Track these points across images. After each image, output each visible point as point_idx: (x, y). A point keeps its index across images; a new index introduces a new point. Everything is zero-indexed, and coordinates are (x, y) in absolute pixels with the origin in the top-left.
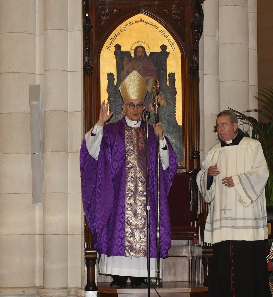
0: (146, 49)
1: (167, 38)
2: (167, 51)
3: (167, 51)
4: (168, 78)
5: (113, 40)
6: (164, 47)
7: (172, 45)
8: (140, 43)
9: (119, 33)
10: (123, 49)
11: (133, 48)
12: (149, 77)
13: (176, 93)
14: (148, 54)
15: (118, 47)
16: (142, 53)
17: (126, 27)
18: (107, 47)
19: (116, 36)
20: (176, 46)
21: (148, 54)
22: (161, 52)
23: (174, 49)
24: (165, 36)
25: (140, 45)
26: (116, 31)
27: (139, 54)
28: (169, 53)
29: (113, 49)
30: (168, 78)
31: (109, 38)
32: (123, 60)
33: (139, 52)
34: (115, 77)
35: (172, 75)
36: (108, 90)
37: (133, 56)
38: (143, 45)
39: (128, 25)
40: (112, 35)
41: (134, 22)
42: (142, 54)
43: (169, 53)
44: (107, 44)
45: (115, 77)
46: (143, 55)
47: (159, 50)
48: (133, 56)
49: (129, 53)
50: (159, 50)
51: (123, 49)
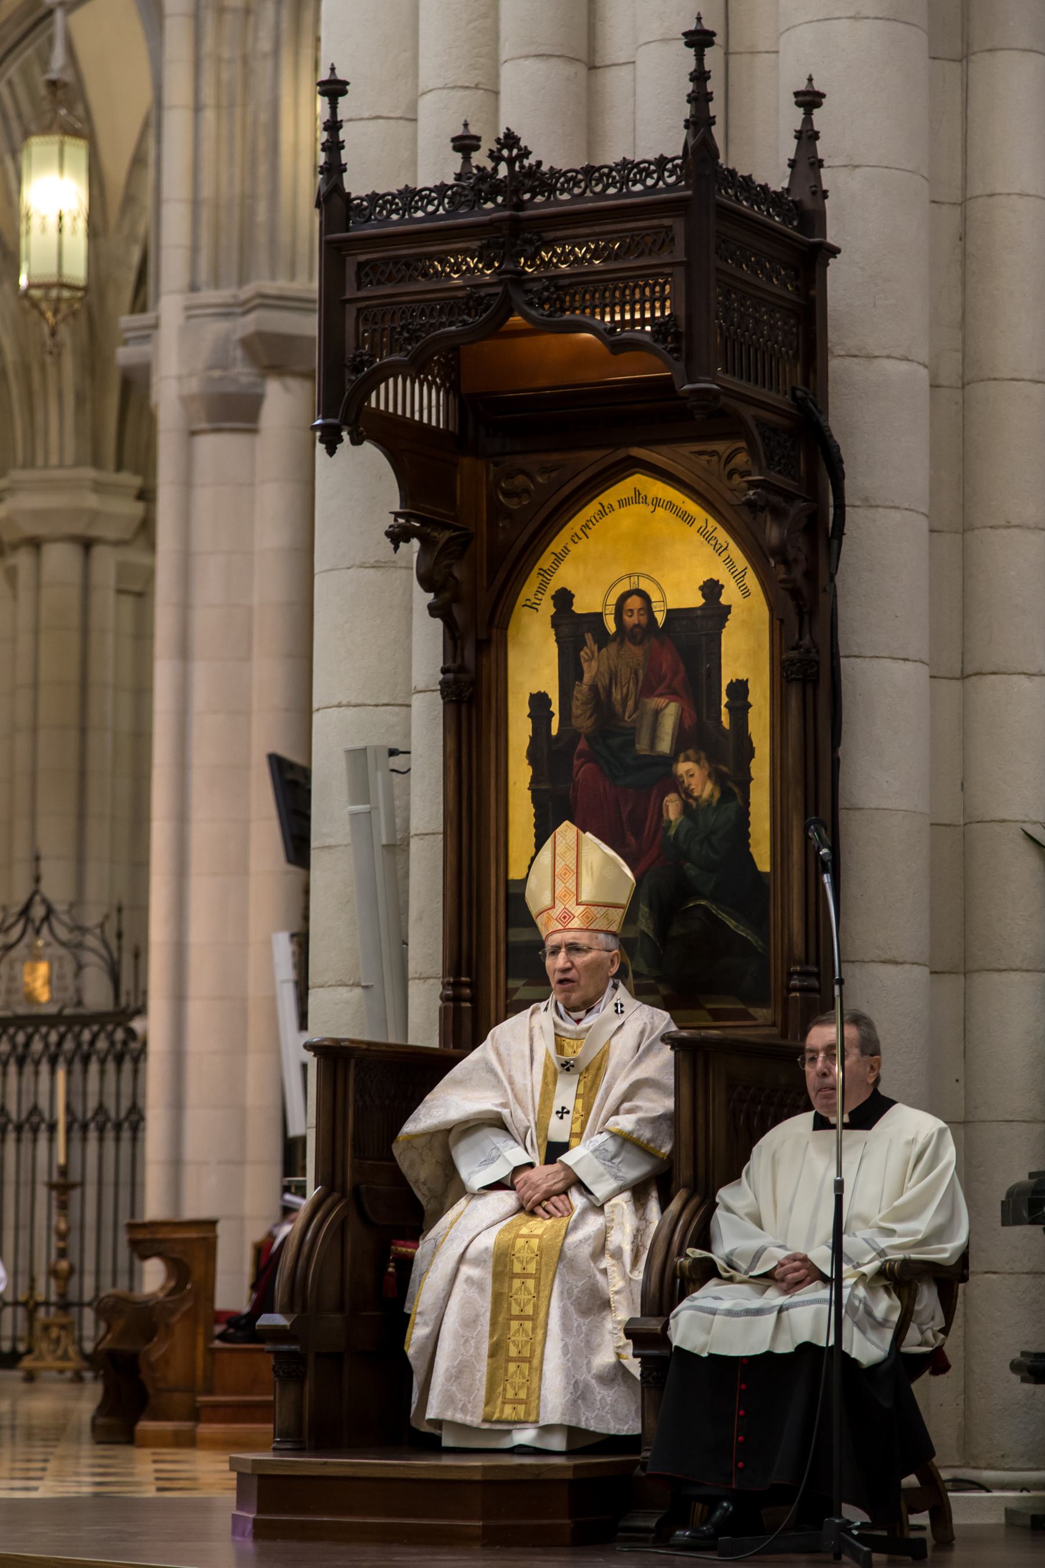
0: (655, 596)
1: (724, 555)
2: (723, 600)
3: (723, 600)
4: (725, 699)
5: (546, 575)
6: (712, 589)
7: (739, 578)
8: (634, 579)
9: (566, 550)
10: (580, 607)
11: (613, 600)
12: (661, 702)
13: (751, 753)
14: (660, 618)
15: (563, 598)
16: (642, 615)
17: (591, 525)
18: (529, 603)
19: (559, 559)
20: (752, 580)
21: (660, 618)
22: (701, 608)
23: (746, 593)
24: (717, 547)
25: (633, 587)
26: (556, 546)
27: (630, 621)
28: (728, 609)
29: (548, 608)
30: (725, 699)
31: (536, 570)
32: (580, 644)
33: (631, 611)
34: (555, 708)
35: (740, 689)
36: (533, 756)
37: (611, 626)
38: (645, 585)
39: (597, 517)
40: (545, 561)
41: (616, 505)
42: (641, 618)
43: (728, 609)
44: (528, 591)
45: (555, 708)
46: (644, 620)
47: (695, 600)
48: (611, 626)
49: (597, 618)
50: (695, 600)
51: (580, 607)
